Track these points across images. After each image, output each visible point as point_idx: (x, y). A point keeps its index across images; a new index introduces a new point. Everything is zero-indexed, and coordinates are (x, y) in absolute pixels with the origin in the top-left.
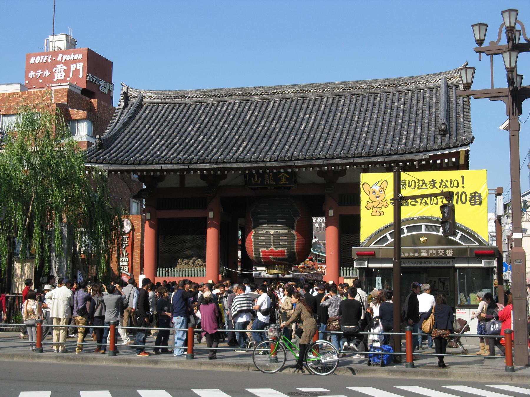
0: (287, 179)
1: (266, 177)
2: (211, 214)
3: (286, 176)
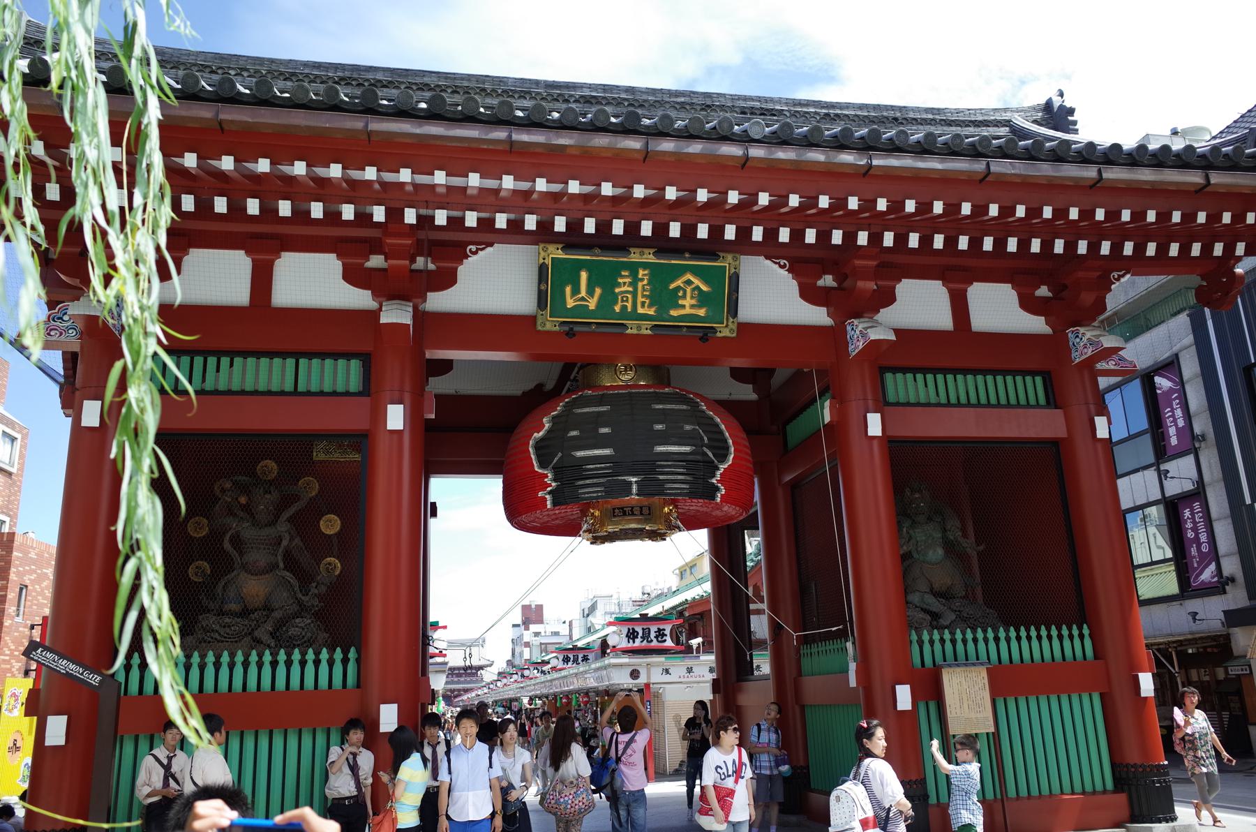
0: (703, 299)
1: (624, 285)
2: (396, 417)
3: (698, 288)
